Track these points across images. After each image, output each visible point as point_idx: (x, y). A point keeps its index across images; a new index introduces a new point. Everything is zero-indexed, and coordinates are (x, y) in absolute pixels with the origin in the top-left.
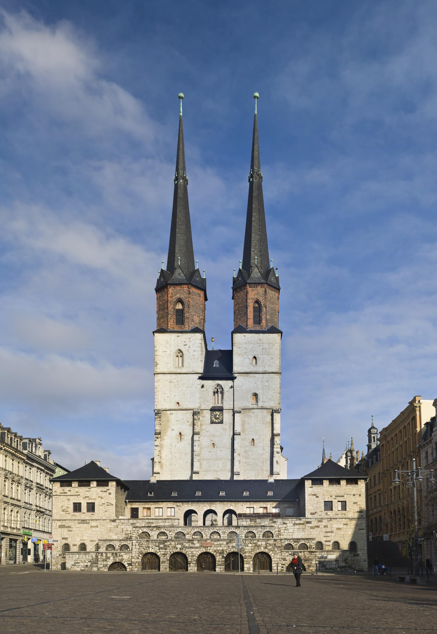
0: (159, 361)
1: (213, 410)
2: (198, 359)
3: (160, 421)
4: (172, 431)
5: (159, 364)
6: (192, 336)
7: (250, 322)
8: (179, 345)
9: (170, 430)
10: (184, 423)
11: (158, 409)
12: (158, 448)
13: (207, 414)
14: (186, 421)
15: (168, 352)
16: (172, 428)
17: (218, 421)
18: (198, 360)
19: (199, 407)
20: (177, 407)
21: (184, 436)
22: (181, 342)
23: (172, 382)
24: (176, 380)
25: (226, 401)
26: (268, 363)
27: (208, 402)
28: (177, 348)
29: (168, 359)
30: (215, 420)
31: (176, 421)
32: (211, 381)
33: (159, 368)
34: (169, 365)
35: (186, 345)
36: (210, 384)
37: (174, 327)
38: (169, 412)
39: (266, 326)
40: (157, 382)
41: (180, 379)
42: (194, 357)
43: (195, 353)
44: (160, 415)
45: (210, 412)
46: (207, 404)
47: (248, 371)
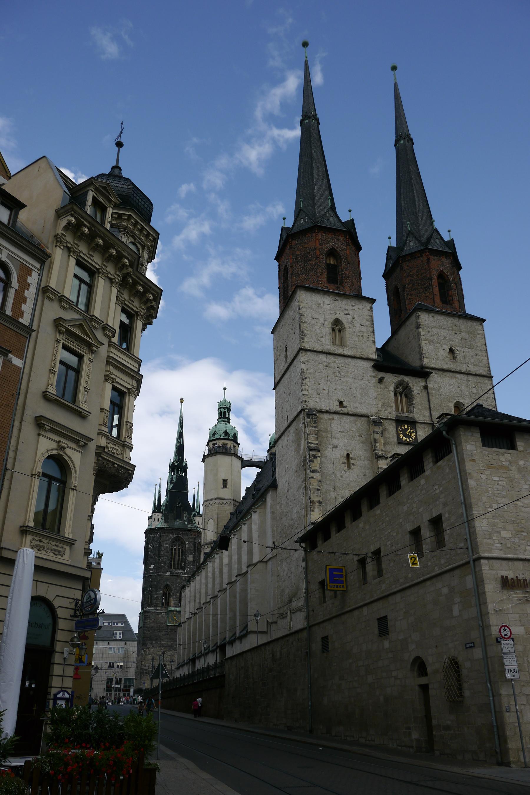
0: (307, 331)
1: (399, 422)
2: (368, 338)
3: (316, 427)
4: (334, 449)
5: (306, 336)
6: (357, 303)
7: (438, 299)
8: (338, 313)
9: (331, 446)
10: (354, 437)
11: (308, 407)
12: (317, 476)
13: (391, 426)
14: (357, 435)
15: (321, 320)
16: (335, 442)
17: (409, 440)
18: (367, 339)
19: (376, 413)
20: (338, 409)
21: (354, 459)
22: (339, 309)
23: (330, 367)
24: (335, 365)
25: (419, 409)
26: (472, 360)
27: (390, 406)
28: (335, 317)
29: (321, 331)
30: (404, 439)
31: (340, 432)
32: (392, 374)
33: (308, 342)
34: (323, 340)
35: (348, 314)
36: (391, 380)
37: (328, 287)
38: (326, 416)
39: (460, 309)
40: (304, 363)
41: (343, 364)
42: (361, 334)
43: (364, 329)
44: (315, 417)
45: (394, 424)
46: (389, 409)
47: (446, 367)
